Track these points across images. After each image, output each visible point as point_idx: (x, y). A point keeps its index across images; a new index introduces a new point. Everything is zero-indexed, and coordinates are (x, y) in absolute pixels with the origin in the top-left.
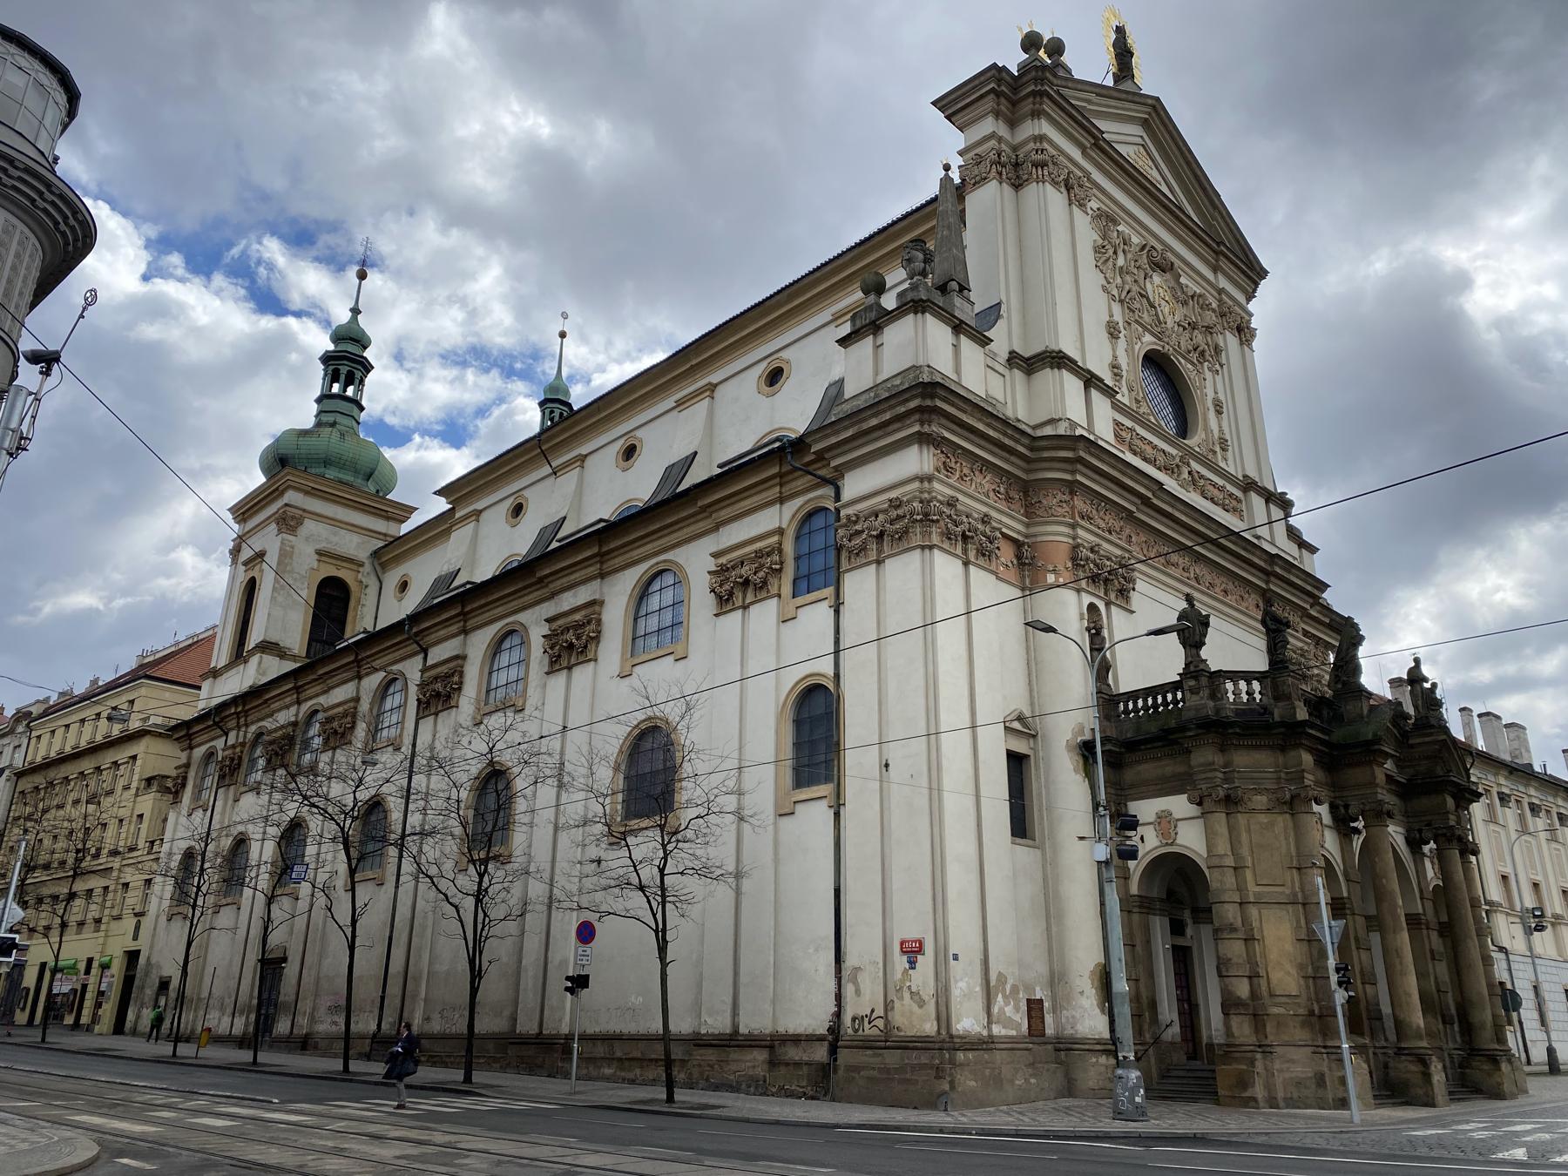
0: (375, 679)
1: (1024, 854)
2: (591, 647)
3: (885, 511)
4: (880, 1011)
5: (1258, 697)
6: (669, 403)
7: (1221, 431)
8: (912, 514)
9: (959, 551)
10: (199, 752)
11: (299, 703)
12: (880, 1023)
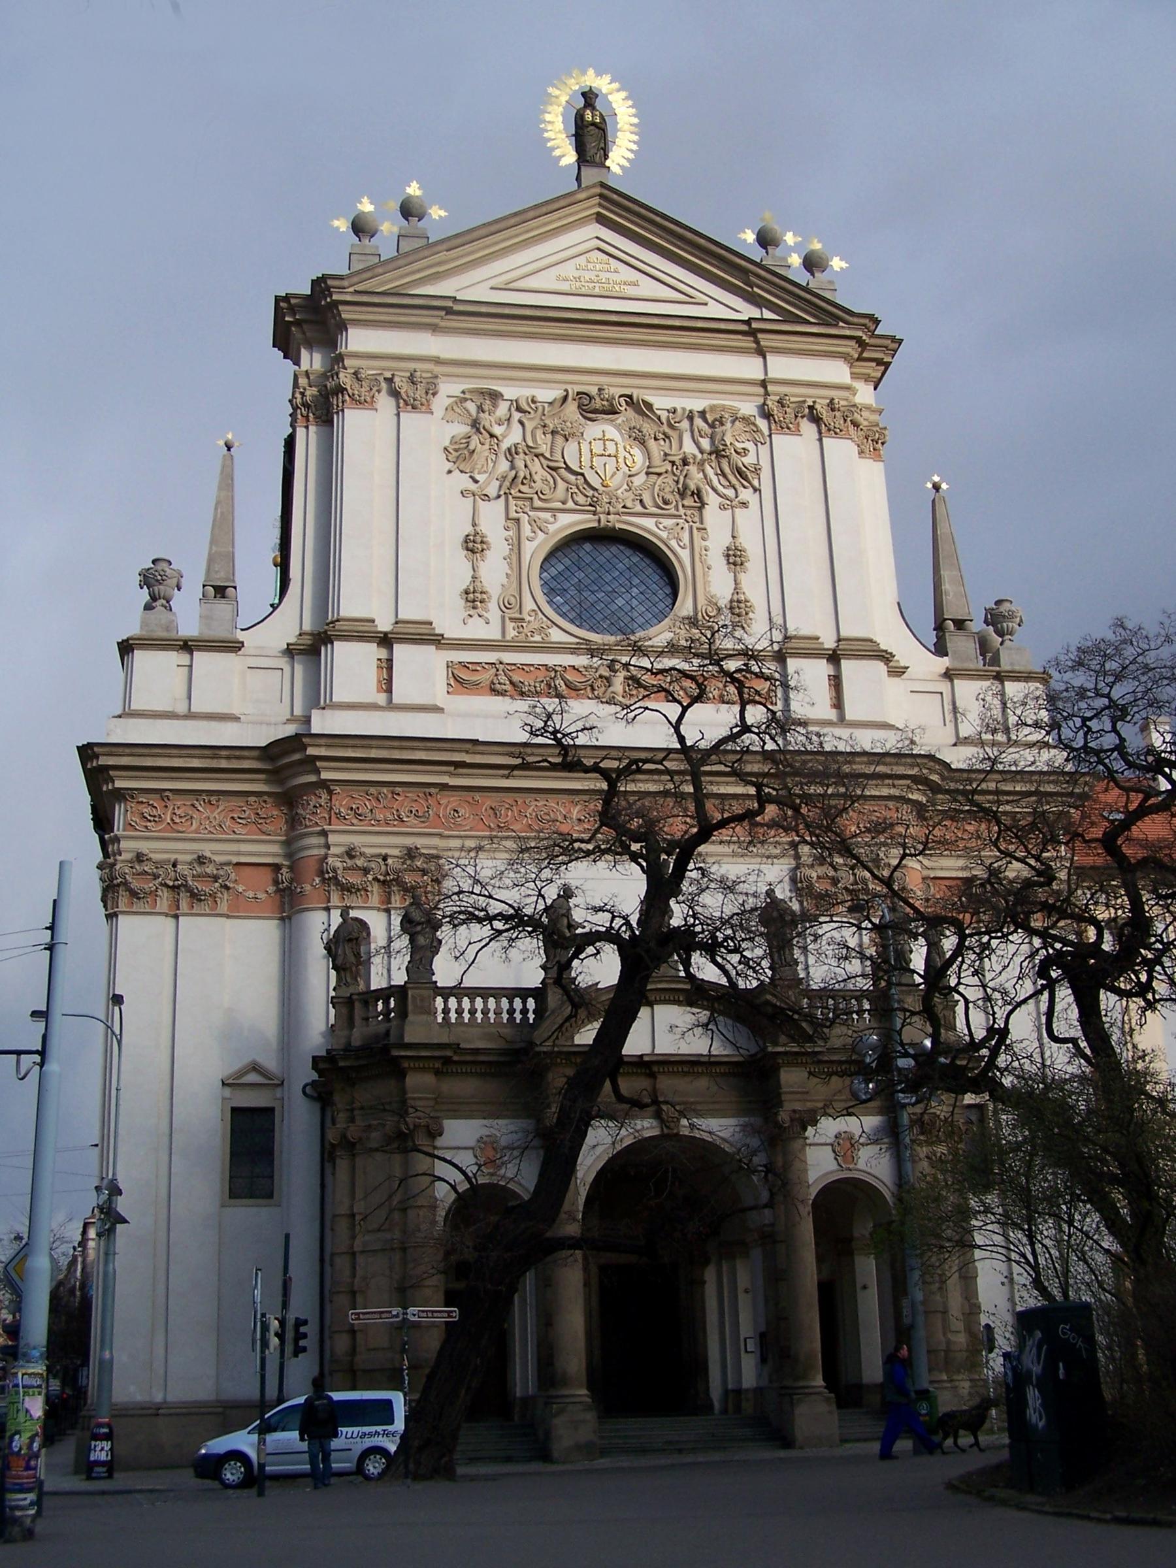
7: (737, 589)
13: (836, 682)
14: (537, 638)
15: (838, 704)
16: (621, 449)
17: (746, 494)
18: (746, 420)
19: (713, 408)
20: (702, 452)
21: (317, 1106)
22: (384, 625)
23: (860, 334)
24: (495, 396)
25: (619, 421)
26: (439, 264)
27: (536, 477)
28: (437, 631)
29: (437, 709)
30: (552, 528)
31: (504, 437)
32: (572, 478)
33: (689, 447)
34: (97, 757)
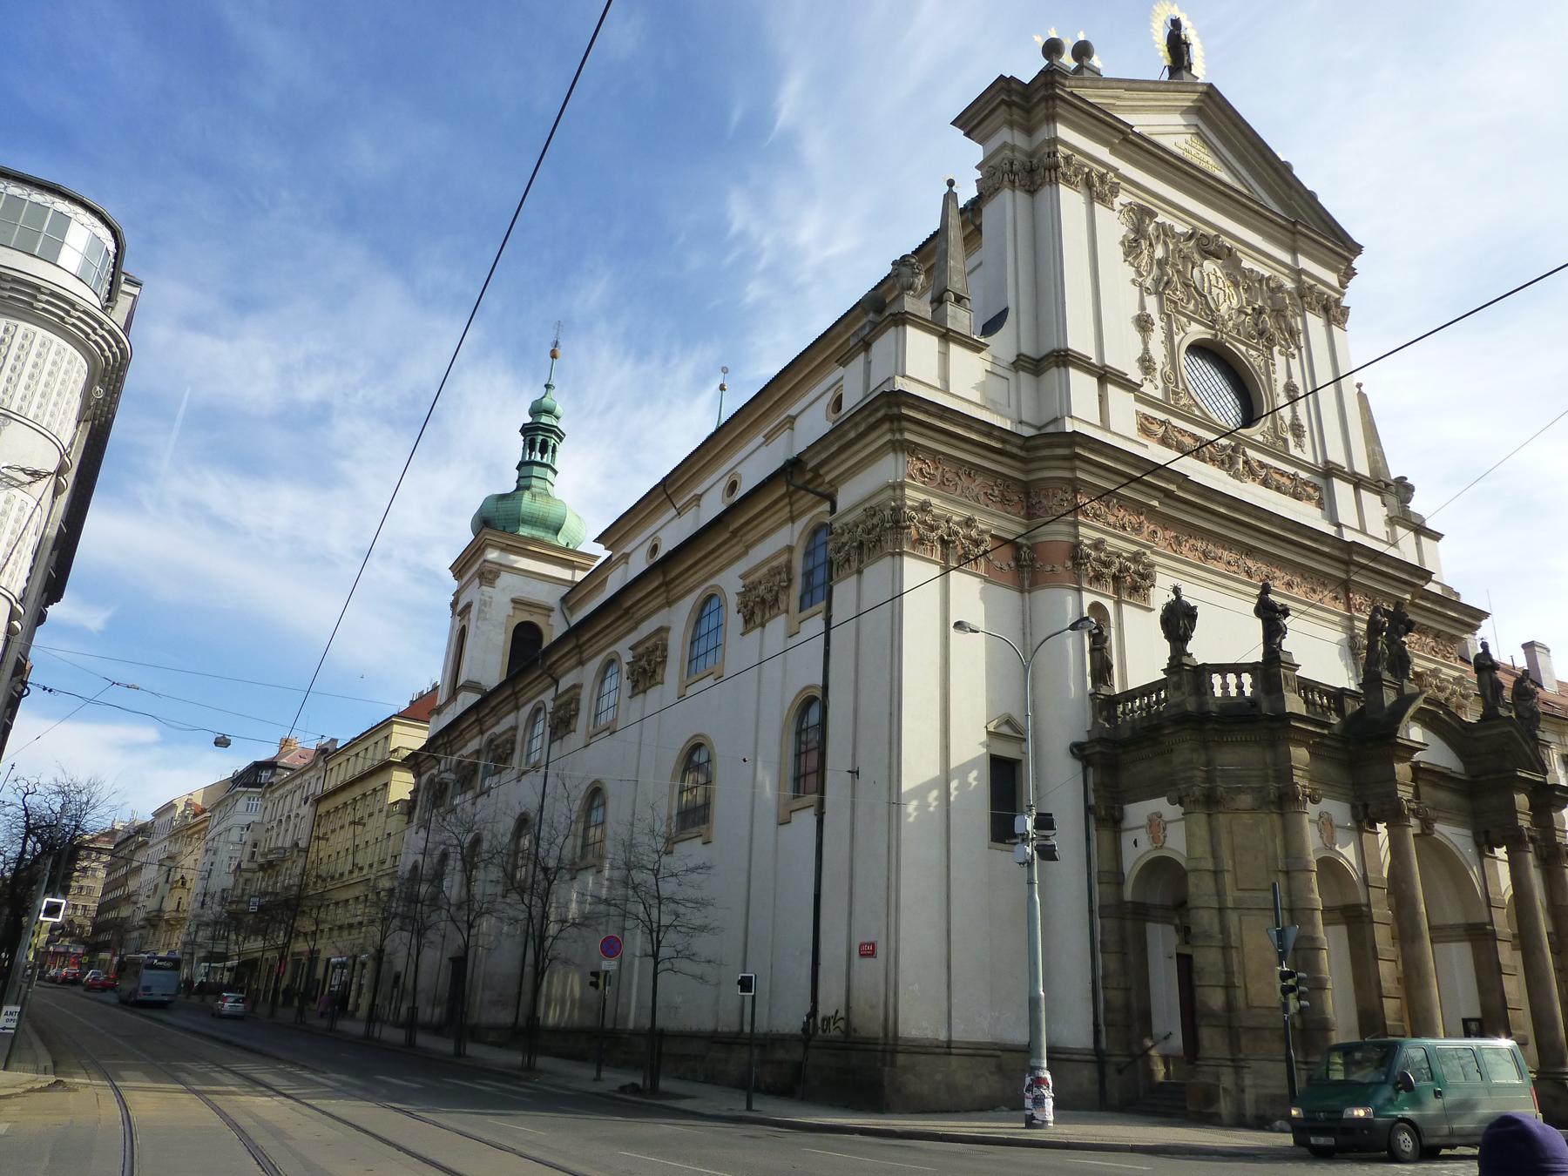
0: (526, 711)
1: (1005, 859)
2: (659, 671)
3: (864, 522)
4: (842, 1013)
5: (1248, 691)
6: (760, 439)
8: (883, 521)
9: (937, 557)
10: (425, 778)
11: (482, 732)
12: (841, 1024)
21: (1078, 765)
24: (1153, 215)
26: (1118, 98)
34: (899, 406)
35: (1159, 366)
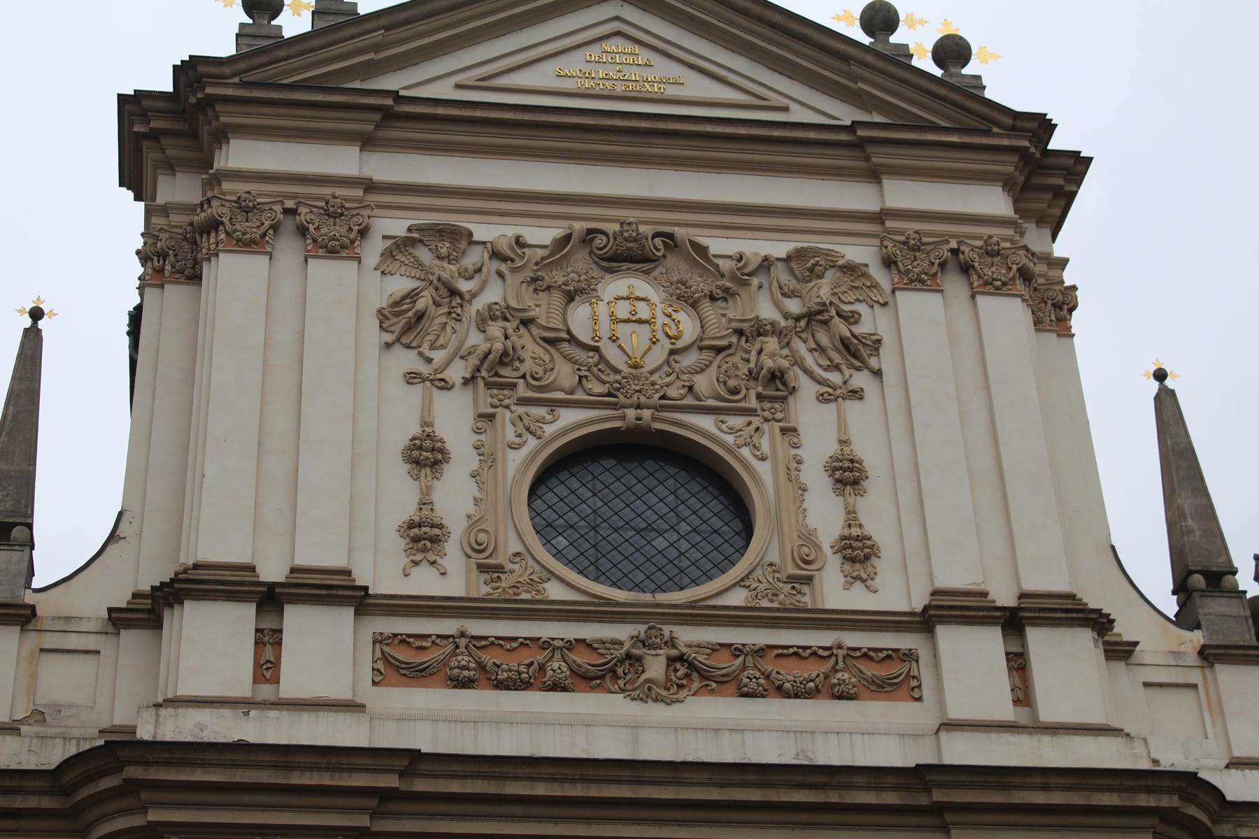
7: (851, 516)
13: (1018, 663)
14: (525, 596)
15: (1023, 695)
16: (659, 314)
17: (860, 379)
18: (851, 269)
19: (799, 255)
20: (786, 316)
22: (272, 571)
23: (1026, 143)
25: (656, 273)
26: (377, 48)
27: (526, 355)
28: (360, 582)
29: (352, 706)
30: (549, 430)
31: (474, 295)
32: (582, 356)
33: (767, 311)
35: (456, 525)
